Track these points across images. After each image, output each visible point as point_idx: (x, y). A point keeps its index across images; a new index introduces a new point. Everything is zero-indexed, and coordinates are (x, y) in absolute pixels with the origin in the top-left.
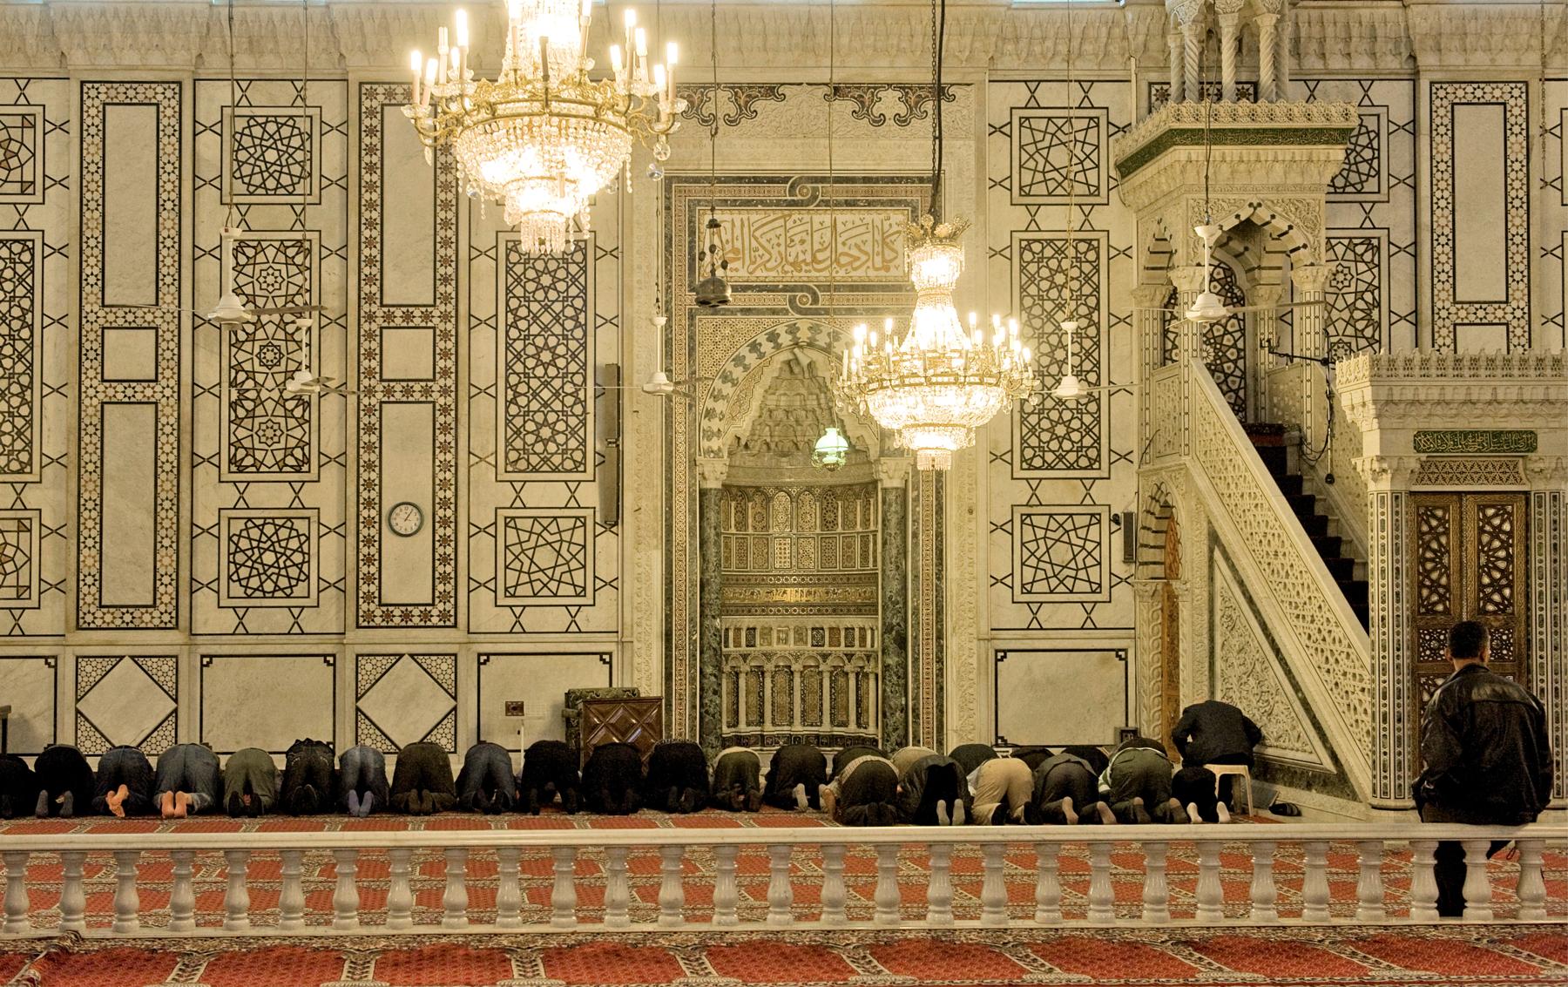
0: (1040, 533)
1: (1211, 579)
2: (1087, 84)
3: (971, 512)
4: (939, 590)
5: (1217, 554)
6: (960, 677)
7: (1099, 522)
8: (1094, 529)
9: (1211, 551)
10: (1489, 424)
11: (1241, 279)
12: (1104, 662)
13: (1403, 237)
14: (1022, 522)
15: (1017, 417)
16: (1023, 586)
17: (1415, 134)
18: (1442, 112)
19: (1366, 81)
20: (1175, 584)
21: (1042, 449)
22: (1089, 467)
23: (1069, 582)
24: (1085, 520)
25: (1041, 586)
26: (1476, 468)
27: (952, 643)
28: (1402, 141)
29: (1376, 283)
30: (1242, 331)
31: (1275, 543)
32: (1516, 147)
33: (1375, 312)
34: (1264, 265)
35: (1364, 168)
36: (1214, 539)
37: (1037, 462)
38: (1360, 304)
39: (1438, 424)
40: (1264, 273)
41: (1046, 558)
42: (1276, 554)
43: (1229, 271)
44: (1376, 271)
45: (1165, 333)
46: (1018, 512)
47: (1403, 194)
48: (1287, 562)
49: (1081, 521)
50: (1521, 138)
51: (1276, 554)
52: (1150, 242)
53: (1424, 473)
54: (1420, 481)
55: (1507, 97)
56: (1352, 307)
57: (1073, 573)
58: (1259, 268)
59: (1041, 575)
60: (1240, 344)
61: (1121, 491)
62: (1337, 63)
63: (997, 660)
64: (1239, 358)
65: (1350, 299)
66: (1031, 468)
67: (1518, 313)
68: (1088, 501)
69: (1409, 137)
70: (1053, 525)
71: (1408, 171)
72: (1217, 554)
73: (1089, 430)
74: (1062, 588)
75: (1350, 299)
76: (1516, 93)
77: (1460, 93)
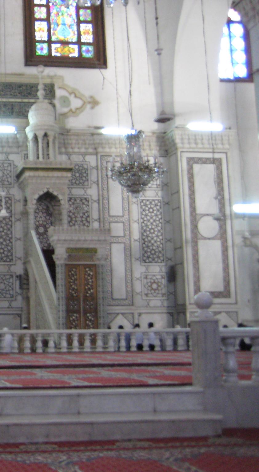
2: (7, 154)
10: (85, 246)
11: (51, 209)
13: (95, 197)
17: (97, 169)
19: (84, 154)
28: (95, 171)
39: (72, 246)
43: (48, 207)
47: (95, 187)
56: (82, 217)
61: (18, 269)
62: (76, 150)
65: (81, 215)
67: (126, 220)
71: (96, 180)
75: (81, 215)
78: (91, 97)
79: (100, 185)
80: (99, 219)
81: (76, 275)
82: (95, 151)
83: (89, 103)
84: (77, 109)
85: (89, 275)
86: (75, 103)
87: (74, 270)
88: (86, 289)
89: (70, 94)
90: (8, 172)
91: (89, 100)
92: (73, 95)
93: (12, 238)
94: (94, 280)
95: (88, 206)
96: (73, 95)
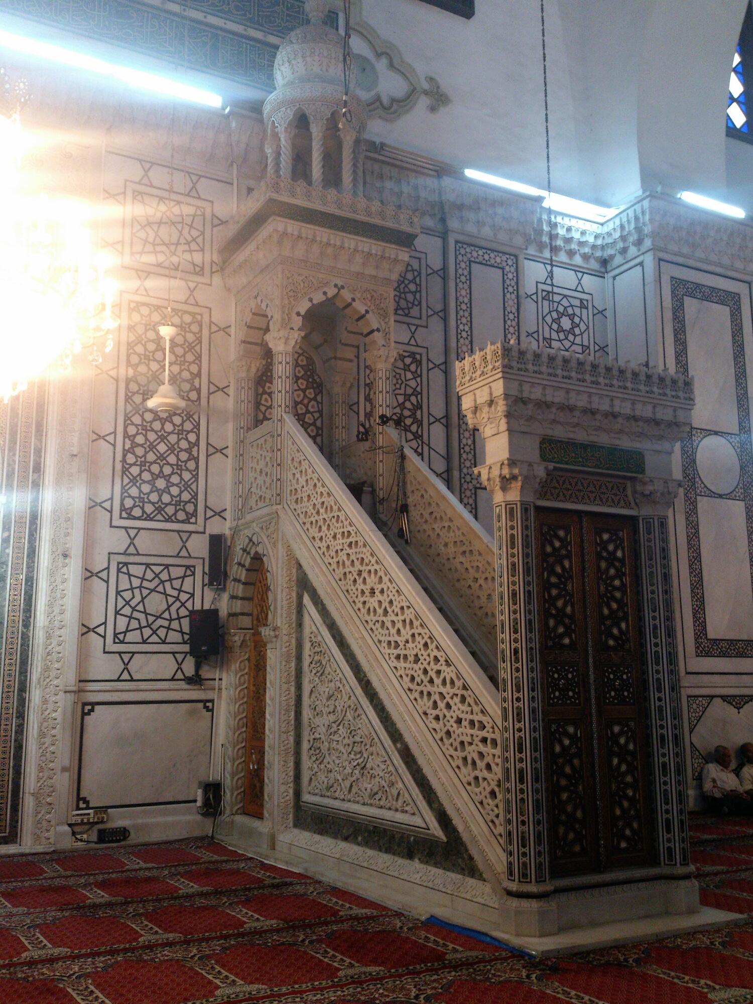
0: (136, 582)
1: (300, 625)
3: (65, 556)
4: (25, 638)
5: (306, 600)
6: (42, 735)
7: (193, 574)
8: (188, 581)
9: (300, 598)
12: (192, 713)
14: (119, 570)
15: (119, 466)
16: (116, 635)
18: (463, 265)
20: (265, 632)
21: (141, 501)
22: (186, 521)
23: (162, 633)
24: (180, 572)
25: (132, 637)
26: (592, 488)
27: (35, 696)
28: (437, 282)
29: (419, 389)
30: (320, 412)
31: (372, 581)
32: (511, 303)
33: (419, 412)
34: (338, 355)
35: (410, 297)
36: (304, 584)
37: (137, 512)
38: (408, 405)
40: (339, 362)
41: (140, 607)
42: (372, 592)
44: (419, 379)
45: (258, 404)
46: (115, 560)
47: (436, 324)
48: (384, 599)
49: (177, 572)
50: (513, 296)
51: (372, 592)
52: (248, 317)
53: (546, 488)
54: (543, 495)
55: (504, 264)
57: (166, 623)
58: (335, 358)
59: (134, 624)
60: (319, 423)
63: (84, 714)
64: (317, 435)
66: (131, 517)
68: (184, 553)
69: (439, 280)
70: (149, 575)
71: (439, 307)
72: (306, 600)
73: (187, 486)
74: (155, 638)
76: (510, 262)
77: (475, 254)
78: (431, 79)
79: (452, 323)
80: (447, 416)
81: (569, 556)
82: (439, 227)
83: (426, 93)
84: (393, 100)
85: (612, 559)
86: (390, 85)
87: (561, 533)
88: (603, 618)
89: (379, 55)
90: (195, 233)
91: (426, 86)
92: (384, 61)
93: (197, 443)
94: (627, 580)
95: (417, 375)
96: (384, 61)
